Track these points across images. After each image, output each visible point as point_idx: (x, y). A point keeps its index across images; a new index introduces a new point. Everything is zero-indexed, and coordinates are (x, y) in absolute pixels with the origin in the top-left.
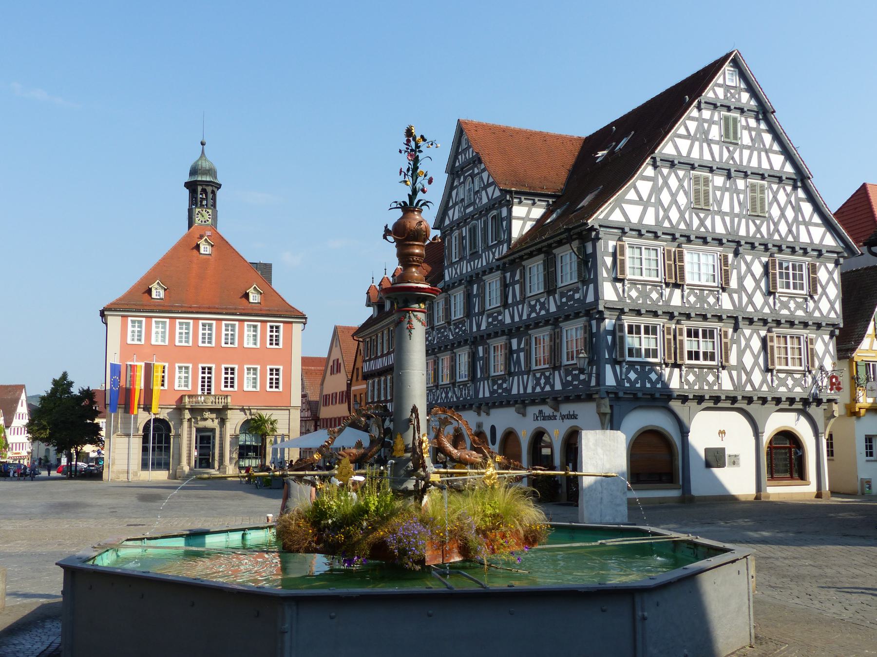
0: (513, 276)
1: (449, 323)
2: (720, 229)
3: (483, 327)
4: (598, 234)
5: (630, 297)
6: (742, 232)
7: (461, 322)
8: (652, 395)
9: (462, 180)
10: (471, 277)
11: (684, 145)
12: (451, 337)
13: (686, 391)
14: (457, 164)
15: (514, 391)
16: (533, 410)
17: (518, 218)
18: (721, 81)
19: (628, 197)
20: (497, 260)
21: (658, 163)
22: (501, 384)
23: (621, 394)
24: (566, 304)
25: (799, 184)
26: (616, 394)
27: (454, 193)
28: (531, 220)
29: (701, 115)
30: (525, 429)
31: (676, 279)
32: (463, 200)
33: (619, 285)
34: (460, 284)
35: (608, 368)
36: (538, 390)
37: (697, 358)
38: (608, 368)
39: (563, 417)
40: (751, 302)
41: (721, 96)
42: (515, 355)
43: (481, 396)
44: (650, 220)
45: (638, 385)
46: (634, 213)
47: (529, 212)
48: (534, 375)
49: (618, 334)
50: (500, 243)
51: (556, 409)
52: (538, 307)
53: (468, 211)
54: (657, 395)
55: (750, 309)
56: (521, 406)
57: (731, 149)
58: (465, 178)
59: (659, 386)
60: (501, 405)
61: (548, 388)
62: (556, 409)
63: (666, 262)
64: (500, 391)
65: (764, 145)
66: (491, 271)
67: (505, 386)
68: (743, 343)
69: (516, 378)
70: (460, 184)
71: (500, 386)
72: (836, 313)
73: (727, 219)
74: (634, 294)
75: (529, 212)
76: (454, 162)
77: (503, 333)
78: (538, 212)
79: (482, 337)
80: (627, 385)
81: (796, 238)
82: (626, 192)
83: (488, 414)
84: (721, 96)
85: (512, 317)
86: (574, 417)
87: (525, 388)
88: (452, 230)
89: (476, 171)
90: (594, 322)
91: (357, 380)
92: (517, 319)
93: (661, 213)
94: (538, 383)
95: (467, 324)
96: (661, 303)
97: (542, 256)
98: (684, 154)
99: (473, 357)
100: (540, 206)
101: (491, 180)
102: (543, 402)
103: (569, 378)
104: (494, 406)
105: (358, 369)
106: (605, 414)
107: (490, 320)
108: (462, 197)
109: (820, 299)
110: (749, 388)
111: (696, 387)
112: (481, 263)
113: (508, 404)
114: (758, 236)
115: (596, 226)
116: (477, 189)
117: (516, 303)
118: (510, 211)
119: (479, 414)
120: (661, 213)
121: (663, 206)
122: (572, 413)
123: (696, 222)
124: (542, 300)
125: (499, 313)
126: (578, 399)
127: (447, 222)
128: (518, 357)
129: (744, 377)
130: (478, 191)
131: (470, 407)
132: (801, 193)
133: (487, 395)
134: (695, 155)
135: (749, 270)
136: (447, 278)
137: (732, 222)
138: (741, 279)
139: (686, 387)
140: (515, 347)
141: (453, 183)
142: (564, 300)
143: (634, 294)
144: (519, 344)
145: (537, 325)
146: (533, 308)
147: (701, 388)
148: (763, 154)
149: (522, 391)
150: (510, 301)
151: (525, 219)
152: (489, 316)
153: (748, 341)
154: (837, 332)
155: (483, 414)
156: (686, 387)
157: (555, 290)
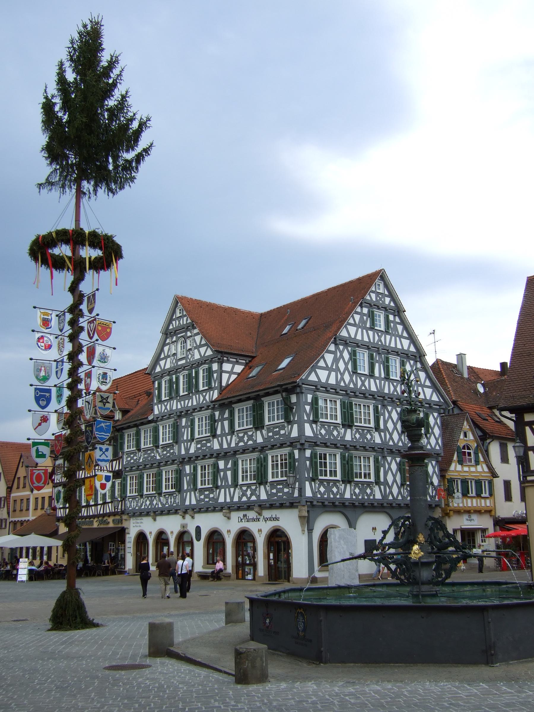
0: (222, 414)
1: (157, 447)
2: (373, 389)
3: (192, 451)
4: (301, 390)
5: (321, 434)
6: (386, 391)
7: (170, 446)
8: (333, 503)
9: (174, 339)
10: (181, 412)
11: (352, 330)
12: (158, 458)
13: (354, 500)
14: (171, 327)
15: (221, 500)
16: (235, 515)
17: (226, 372)
18: (374, 289)
19: (319, 364)
20: (212, 402)
21: (338, 342)
22: (209, 495)
23: (315, 503)
25: (418, 360)
26: (311, 502)
27: (166, 348)
28: (235, 373)
29: (362, 310)
31: (348, 422)
32: (175, 354)
33: (314, 426)
34: (169, 418)
35: (307, 483)
36: (244, 499)
37: (361, 477)
38: (307, 483)
39: (266, 520)
40: (391, 438)
41: (374, 299)
42: (222, 473)
43: (187, 503)
44: (332, 381)
45: (360, 497)
46: (323, 375)
47: (233, 368)
48: (241, 488)
49: (314, 460)
50: (210, 388)
51: (260, 514)
52: (246, 439)
53: (180, 363)
54: (337, 503)
55: (391, 443)
56: (227, 511)
57: (380, 334)
58: (178, 339)
59: (338, 497)
60: (207, 511)
61: (254, 498)
62: (260, 514)
63: (343, 410)
64: (207, 500)
65: (398, 333)
66: (201, 409)
67: (212, 496)
68: (387, 466)
69: (223, 490)
70: (173, 342)
71: (207, 496)
72: (439, 446)
73: (378, 381)
74: (323, 432)
75: (233, 368)
76: (169, 326)
77: (211, 456)
78: (239, 368)
79: (190, 458)
80: (319, 496)
81: (355, 385)
82: (319, 361)
83: (193, 517)
84: (374, 299)
85: (221, 445)
86: (277, 519)
87: (232, 498)
88: (162, 377)
89: (189, 334)
90: (296, 452)
91: (18, 488)
92: (225, 446)
93: (339, 376)
94: (244, 494)
95: (176, 448)
96: (339, 439)
97: (252, 401)
98: (353, 336)
99: (179, 474)
100: (241, 364)
101: (203, 342)
103: (274, 491)
104: (200, 511)
105: (19, 478)
106: (304, 517)
107: (199, 446)
108: (174, 352)
109: (430, 436)
110: (391, 498)
111: (360, 497)
112: (194, 402)
113: (214, 510)
114: (395, 393)
115: (300, 384)
116: (189, 347)
117: (223, 434)
118: (221, 367)
119: (184, 517)
120: (339, 376)
121: (340, 372)
123: (359, 383)
124: (250, 433)
125: (208, 441)
126: (282, 506)
127: (158, 369)
128: (225, 475)
129: (388, 490)
130: (190, 349)
131: (176, 512)
132: (419, 365)
133: (194, 502)
134: (359, 337)
135: (390, 417)
136: (156, 412)
137: (380, 383)
138: (385, 422)
139: (354, 497)
141: (165, 340)
142: (271, 434)
143: (323, 432)
144: (226, 464)
145: (244, 451)
146: (241, 439)
147: (363, 498)
148: (398, 338)
149: (228, 500)
150: (219, 432)
151: (231, 373)
152: (197, 443)
153: (390, 464)
154: (440, 459)
155: (188, 517)
156: (354, 497)
157: (264, 427)
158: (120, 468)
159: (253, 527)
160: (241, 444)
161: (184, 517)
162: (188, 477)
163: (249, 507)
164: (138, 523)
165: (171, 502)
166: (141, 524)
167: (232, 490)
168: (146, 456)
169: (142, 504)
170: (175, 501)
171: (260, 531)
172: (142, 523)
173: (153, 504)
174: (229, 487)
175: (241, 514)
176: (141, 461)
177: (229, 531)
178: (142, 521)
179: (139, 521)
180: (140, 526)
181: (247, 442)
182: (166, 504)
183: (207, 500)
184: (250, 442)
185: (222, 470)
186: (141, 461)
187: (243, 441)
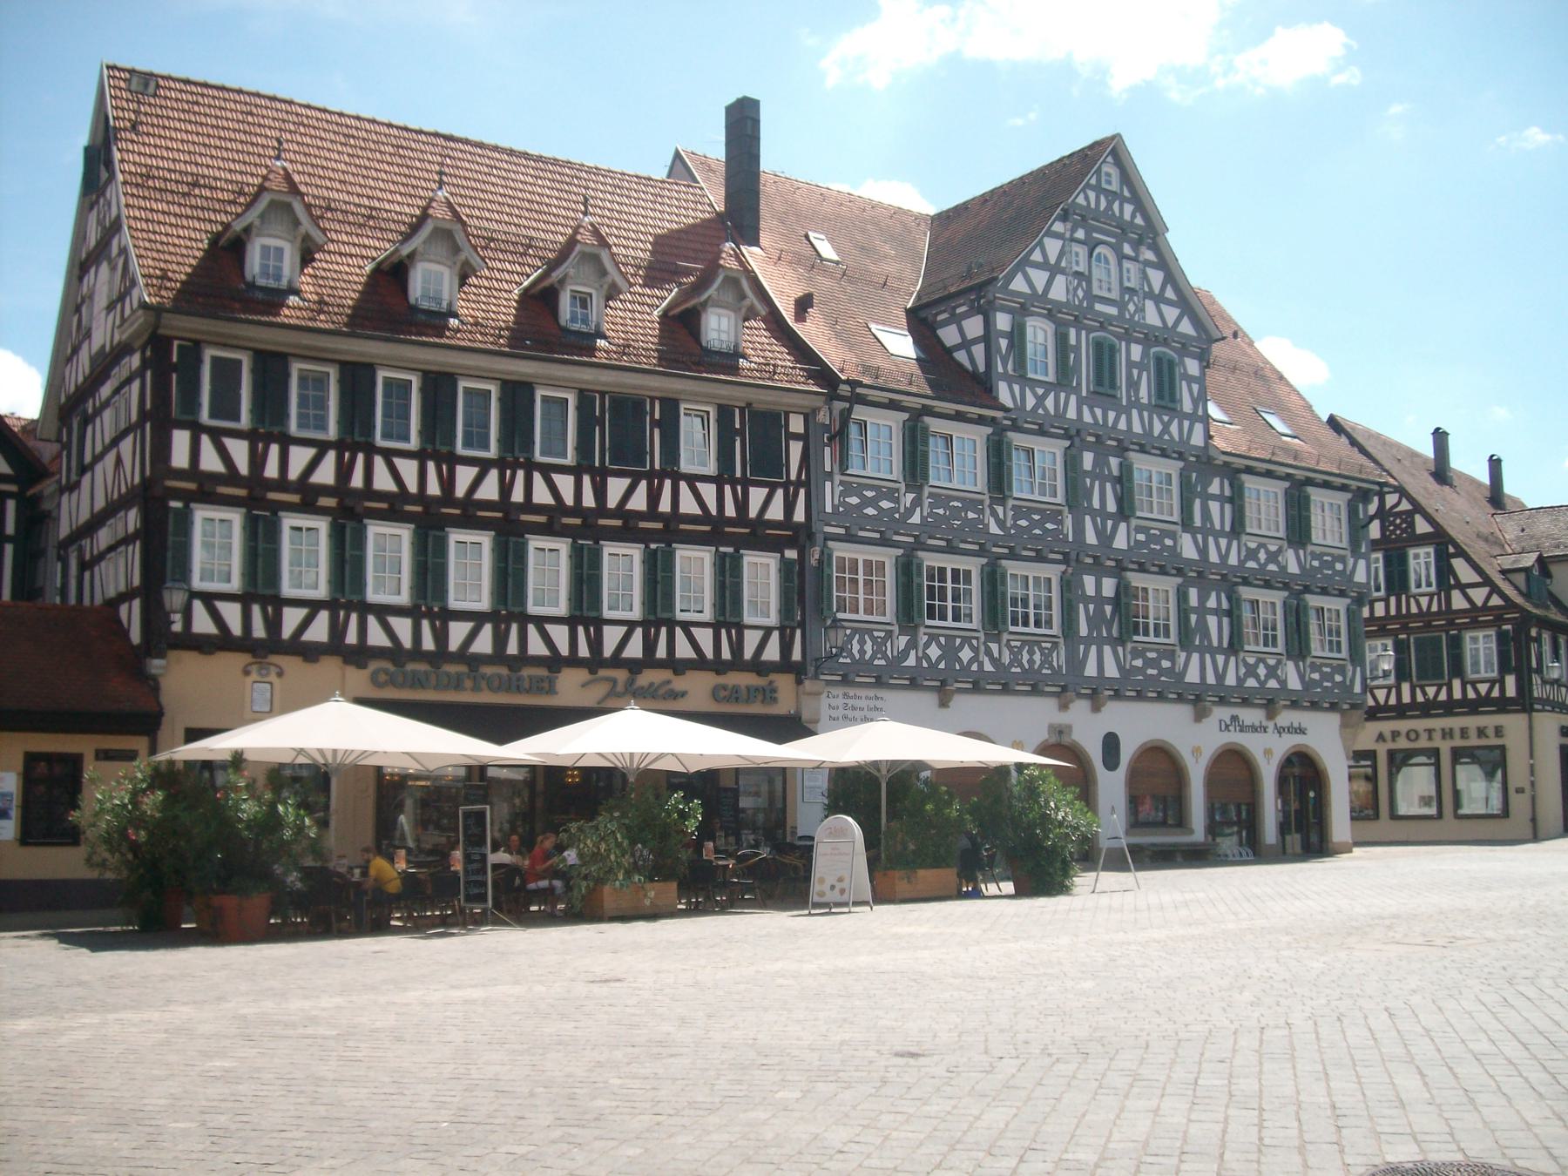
12: (994, 529)
15: (1192, 676)
24: (1319, 570)
30: (1196, 741)
36: (1251, 683)
43: (1091, 670)
52: (1262, 556)
64: (1150, 671)
83: (1096, 708)
86: (1301, 731)
87: (1221, 677)
102: (1246, 702)
104: (1118, 695)
117: (1207, 530)
119: (1064, 707)
122: (1296, 725)
124: (1273, 548)
126: (1315, 706)
133: (1111, 671)
140: (1193, 601)
144: (1203, 598)
158: (799, 516)
159: (1254, 744)
160: (1251, 564)
161: (1064, 707)
162: (1091, 607)
164: (854, 708)
167: (1220, 659)
168: (941, 511)
169: (904, 654)
170: (1046, 660)
172: (876, 709)
174: (1213, 652)
176: (916, 519)
178: (879, 704)
179: (862, 703)
181: (1266, 564)
182: (1011, 664)
183: (1154, 672)
184: (1272, 567)
185: (1195, 610)
186: (916, 519)
187: (1257, 560)
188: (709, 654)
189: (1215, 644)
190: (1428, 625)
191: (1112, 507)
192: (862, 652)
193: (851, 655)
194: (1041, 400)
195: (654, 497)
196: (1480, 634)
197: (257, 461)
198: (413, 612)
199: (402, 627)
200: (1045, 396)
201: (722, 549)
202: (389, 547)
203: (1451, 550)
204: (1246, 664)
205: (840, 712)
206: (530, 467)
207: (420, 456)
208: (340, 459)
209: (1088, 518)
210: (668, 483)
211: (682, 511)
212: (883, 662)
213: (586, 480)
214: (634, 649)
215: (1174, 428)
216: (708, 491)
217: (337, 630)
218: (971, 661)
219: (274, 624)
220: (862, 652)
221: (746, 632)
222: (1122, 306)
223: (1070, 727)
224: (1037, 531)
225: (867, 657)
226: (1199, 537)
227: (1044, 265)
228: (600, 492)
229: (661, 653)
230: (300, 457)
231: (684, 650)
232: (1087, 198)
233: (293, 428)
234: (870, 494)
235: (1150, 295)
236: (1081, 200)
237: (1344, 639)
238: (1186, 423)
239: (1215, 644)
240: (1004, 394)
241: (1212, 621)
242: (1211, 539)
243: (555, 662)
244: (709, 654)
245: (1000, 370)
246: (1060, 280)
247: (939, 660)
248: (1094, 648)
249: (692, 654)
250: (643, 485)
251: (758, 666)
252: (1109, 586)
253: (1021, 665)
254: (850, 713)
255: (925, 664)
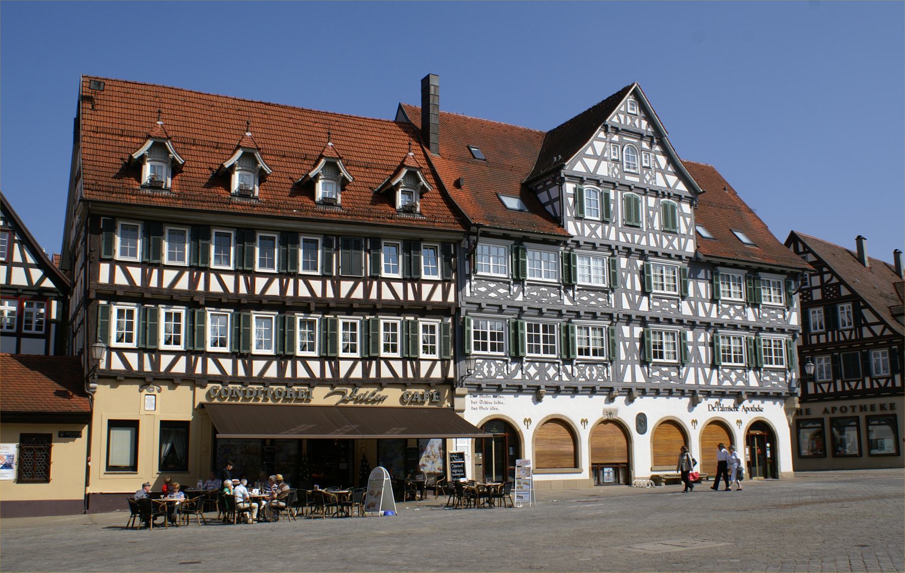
12: (567, 302)
15: (690, 380)
36: (727, 383)
53: (627, 178)
60: (657, 393)
64: (664, 378)
77: (680, 322)
87: (708, 381)
122: (756, 406)
144: (696, 337)
149: (702, 382)
158: (451, 298)
159: (730, 418)
162: (627, 344)
163: (722, 394)
164: (486, 403)
165: (591, 375)
166: (496, 406)
168: (535, 294)
171: (739, 422)
173: (548, 376)
175: (712, 401)
177: (694, 422)
178: (501, 400)
180: (493, 408)
182: (579, 377)
183: (667, 379)
184: (738, 318)
185: (691, 344)
187: (729, 315)
188: (400, 375)
189: (704, 362)
190: (850, 347)
191: (638, 288)
192: (489, 372)
193: (483, 374)
194: (593, 231)
195: (367, 291)
196: (880, 352)
197: (146, 278)
198: (234, 356)
199: (227, 364)
200: (596, 228)
201: (408, 318)
202: (215, 324)
203: (862, 304)
204: (724, 373)
205: (478, 405)
206: (297, 277)
207: (236, 273)
208: (191, 276)
209: (624, 294)
210: (375, 283)
211: (383, 298)
212: (502, 377)
213: (329, 282)
214: (357, 373)
215: (675, 243)
216: (398, 287)
217: (190, 366)
218: (554, 376)
219: (156, 364)
220: (489, 372)
221: (422, 362)
222: (642, 177)
223: (616, 411)
224: (593, 303)
225: (493, 375)
226: (693, 303)
227: (594, 156)
228: (337, 290)
229: (373, 375)
230: (169, 276)
231: (386, 373)
232: (619, 119)
233: (166, 261)
234: (492, 285)
235: (659, 169)
236: (615, 120)
237: (784, 357)
238: (683, 240)
239: (704, 362)
240: (571, 228)
241: (702, 349)
242: (700, 304)
243: (311, 382)
244: (400, 375)
245: (569, 215)
246: (604, 164)
247: (535, 375)
248: (629, 366)
249: (390, 375)
250: (361, 284)
251: (427, 383)
252: (638, 330)
253: (585, 377)
254: (484, 406)
255: (527, 378)
